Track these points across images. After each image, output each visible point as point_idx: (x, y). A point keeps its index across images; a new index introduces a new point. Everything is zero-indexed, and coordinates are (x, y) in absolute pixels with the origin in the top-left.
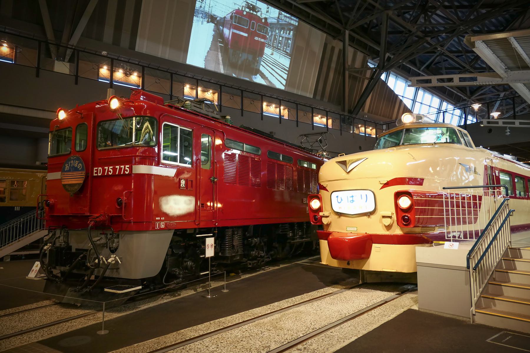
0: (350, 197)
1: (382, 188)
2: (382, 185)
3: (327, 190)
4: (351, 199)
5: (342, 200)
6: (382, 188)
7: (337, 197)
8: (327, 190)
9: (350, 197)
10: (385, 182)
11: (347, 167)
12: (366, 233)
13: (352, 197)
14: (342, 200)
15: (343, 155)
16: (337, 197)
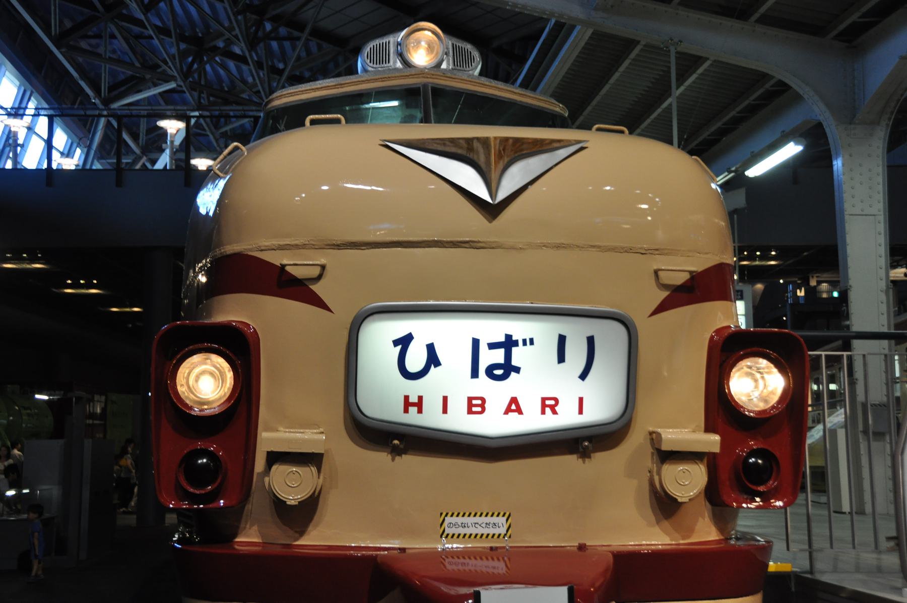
0: (492, 346)
1: (661, 308)
2: (665, 294)
3: (318, 302)
4: (498, 356)
5: (433, 359)
6: (661, 308)
7: (404, 342)
8: (318, 302)
9: (492, 346)
10: (681, 279)
11: (494, 176)
12: (582, 547)
13: (509, 344)
14: (433, 359)
15: (337, 121)
16: (404, 342)
